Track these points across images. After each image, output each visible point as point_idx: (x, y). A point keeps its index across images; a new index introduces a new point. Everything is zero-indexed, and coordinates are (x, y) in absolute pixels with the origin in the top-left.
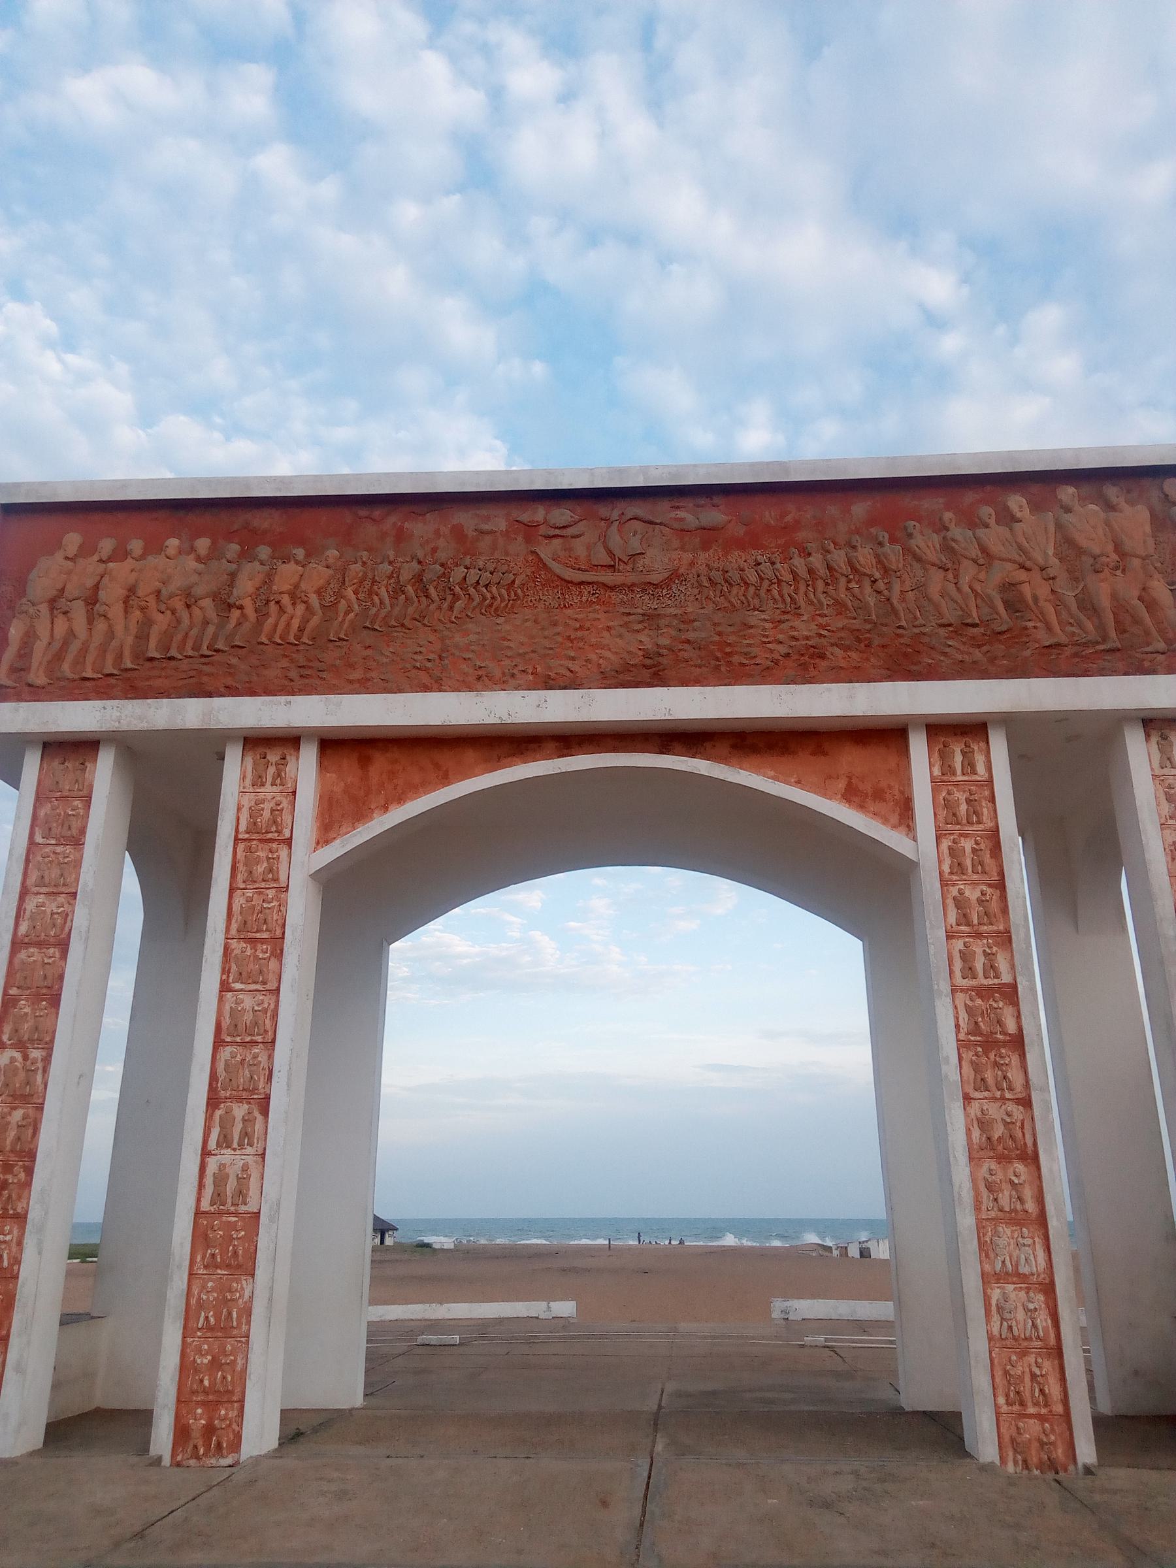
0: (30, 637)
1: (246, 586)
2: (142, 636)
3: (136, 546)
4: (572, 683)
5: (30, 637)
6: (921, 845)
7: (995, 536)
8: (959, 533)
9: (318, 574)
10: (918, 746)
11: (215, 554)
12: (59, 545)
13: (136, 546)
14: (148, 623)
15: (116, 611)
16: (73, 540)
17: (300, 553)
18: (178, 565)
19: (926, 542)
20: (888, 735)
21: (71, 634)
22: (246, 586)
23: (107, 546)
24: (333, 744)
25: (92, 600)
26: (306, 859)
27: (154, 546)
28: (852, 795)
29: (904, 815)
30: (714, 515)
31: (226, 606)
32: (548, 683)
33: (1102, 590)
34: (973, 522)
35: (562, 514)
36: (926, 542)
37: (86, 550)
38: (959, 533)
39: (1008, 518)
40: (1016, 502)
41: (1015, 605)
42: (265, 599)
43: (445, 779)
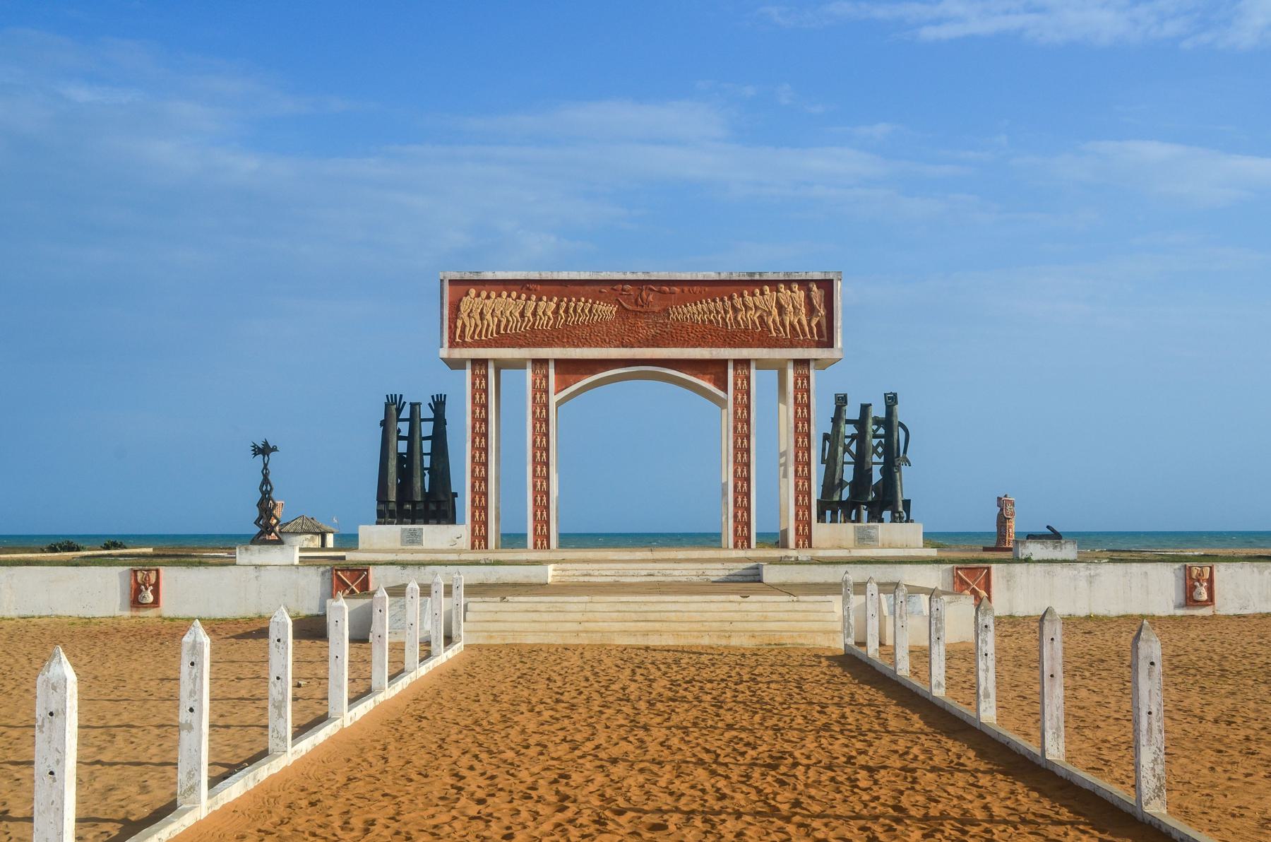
0: (464, 326)
2: (498, 326)
3: (493, 295)
5: (464, 326)
7: (758, 299)
8: (749, 299)
9: (553, 305)
10: (731, 365)
11: (519, 297)
12: (467, 294)
13: (493, 295)
14: (499, 321)
15: (489, 316)
16: (473, 292)
17: (545, 298)
19: (738, 302)
20: (724, 362)
21: (476, 325)
23: (484, 294)
24: (561, 364)
25: (481, 313)
26: (553, 399)
35: (628, 287)
37: (478, 295)
38: (749, 299)
39: (762, 293)
40: (767, 288)
42: (534, 314)
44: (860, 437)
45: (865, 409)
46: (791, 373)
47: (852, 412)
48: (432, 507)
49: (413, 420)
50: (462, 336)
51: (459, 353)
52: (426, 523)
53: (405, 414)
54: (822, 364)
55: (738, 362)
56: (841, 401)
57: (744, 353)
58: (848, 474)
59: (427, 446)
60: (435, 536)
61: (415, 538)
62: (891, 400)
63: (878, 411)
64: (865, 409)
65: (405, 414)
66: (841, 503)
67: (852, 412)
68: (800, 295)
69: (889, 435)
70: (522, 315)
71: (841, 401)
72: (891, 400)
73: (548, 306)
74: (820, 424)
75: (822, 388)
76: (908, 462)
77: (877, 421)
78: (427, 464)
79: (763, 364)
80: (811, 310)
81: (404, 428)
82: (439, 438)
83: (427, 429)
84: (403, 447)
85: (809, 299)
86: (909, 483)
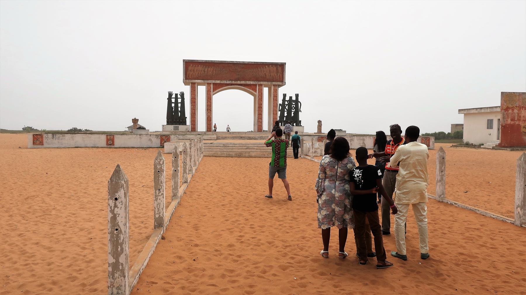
1: (206, 70)
4: (232, 80)
6: (257, 94)
7: (264, 69)
9: (212, 69)
18: (200, 68)
22: (206, 70)
27: (198, 66)
28: (252, 90)
29: (256, 91)
30: (244, 66)
31: (204, 71)
32: (230, 80)
33: (272, 74)
34: (263, 68)
36: (259, 69)
41: (265, 75)
43: (223, 87)
44: (290, 104)
45: (291, 98)
46: (272, 87)
47: (287, 98)
48: (181, 121)
49: (176, 98)
50: (189, 76)
51: (187, 81)
52: (180, 125)
53: (174, 96)
54: (280, 86)
55: (259, 85)
56: (285, 95)
57: (261, 83)
58: (286, 114)
59: (179, 105)
60: (181, 128)
61: (177, 129)
62: (297, 96)
63: (294, 98)
64: (291, 98)
65: (174, 96)
66: (284, 121)
67: (287, 98)
68: (275, 68)
69: (297, 105)
70: (204, 71)
71: (285, 95)
72: (297, 96)
73: (211, 69)
74: (280, 102)
75: (281, 91)
76: (301, 111)
77: (294, 101)
78: (179, 110)
79: (265, 86)
80: (277, 72)
81: (173, 100)
82: (183, 103)
83: (180, 100)
84: (173, 105)
85: (277, 69)
86: (302, 117)
